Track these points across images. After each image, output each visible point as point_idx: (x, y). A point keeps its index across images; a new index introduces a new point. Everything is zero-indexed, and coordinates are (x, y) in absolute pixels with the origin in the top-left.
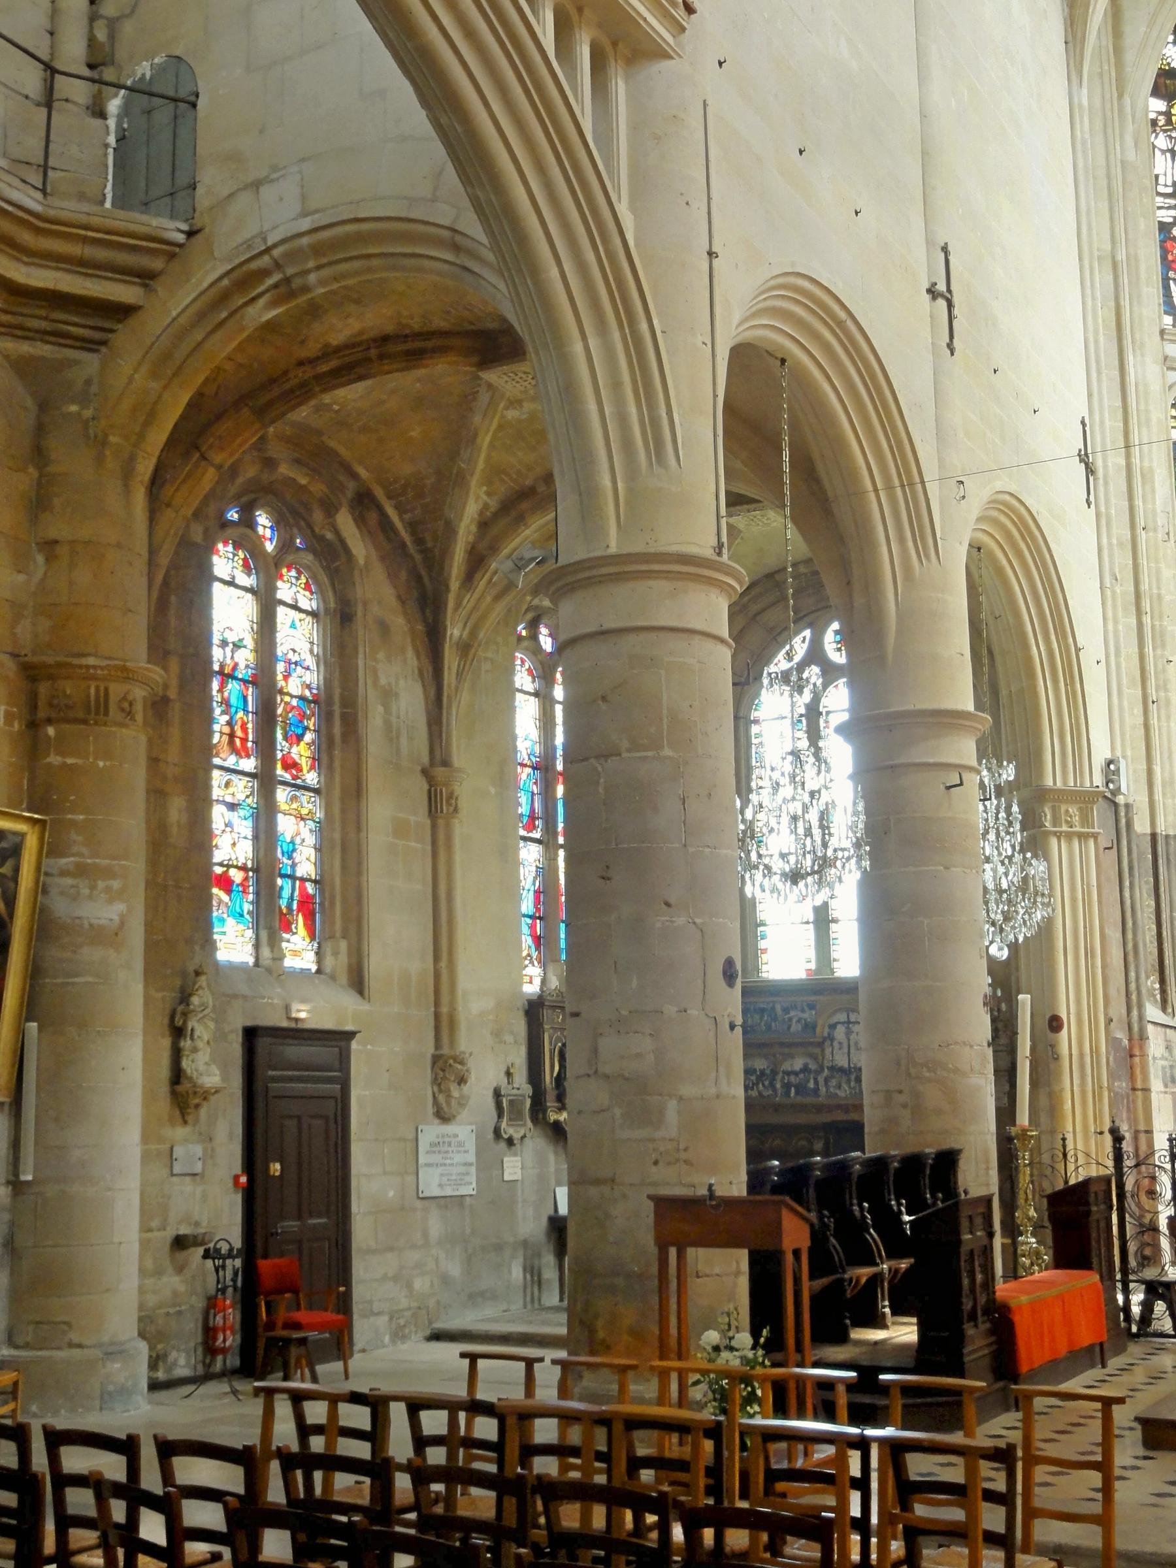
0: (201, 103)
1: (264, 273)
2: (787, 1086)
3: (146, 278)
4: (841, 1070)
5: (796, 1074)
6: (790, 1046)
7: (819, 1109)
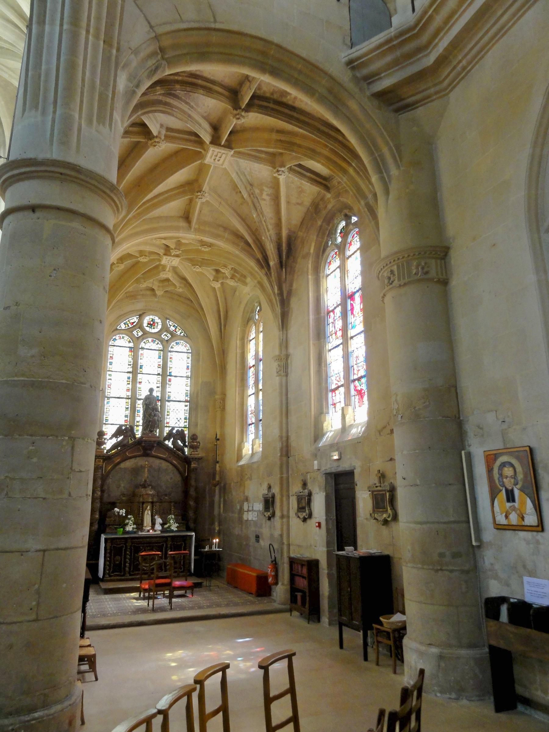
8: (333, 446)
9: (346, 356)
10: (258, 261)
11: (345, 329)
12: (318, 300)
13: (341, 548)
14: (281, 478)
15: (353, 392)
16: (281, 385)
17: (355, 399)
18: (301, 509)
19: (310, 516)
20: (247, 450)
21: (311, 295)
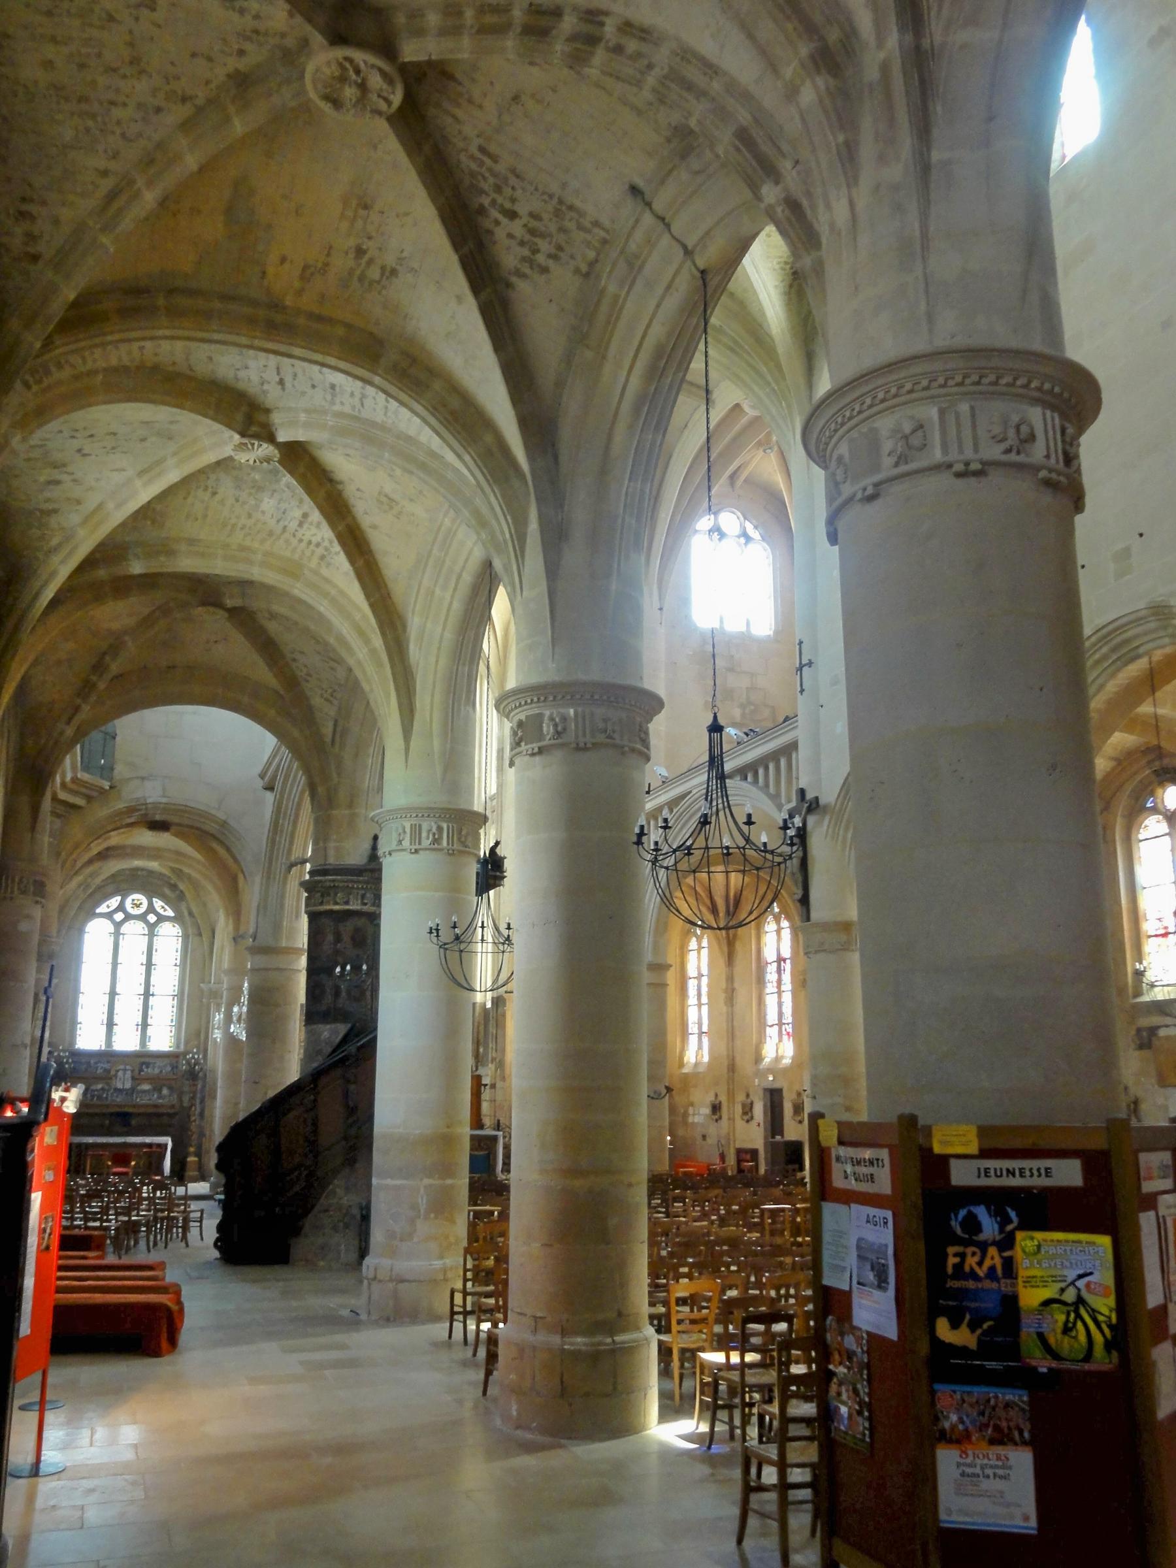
0: (118, 738)
1: (140, 810)
2: (93, 1096)
3: (89, 799)
4: (120, 1090)
5: (97, 1090)
6: (98, 1079)
7: (108, 1106)
8: (770, 1070)
9: (780, 1004)
10: (708, 908)
11: (779, 982)
12: (759, 951)
13: (773, 1137)
14: (728, 1089)
15: (784, 1032)
16: (728, 1013)
17: (785, 1037)
18: (745, 1113)
19: (752, 1118)
20: (690, 1056)
21: (753, 947)
